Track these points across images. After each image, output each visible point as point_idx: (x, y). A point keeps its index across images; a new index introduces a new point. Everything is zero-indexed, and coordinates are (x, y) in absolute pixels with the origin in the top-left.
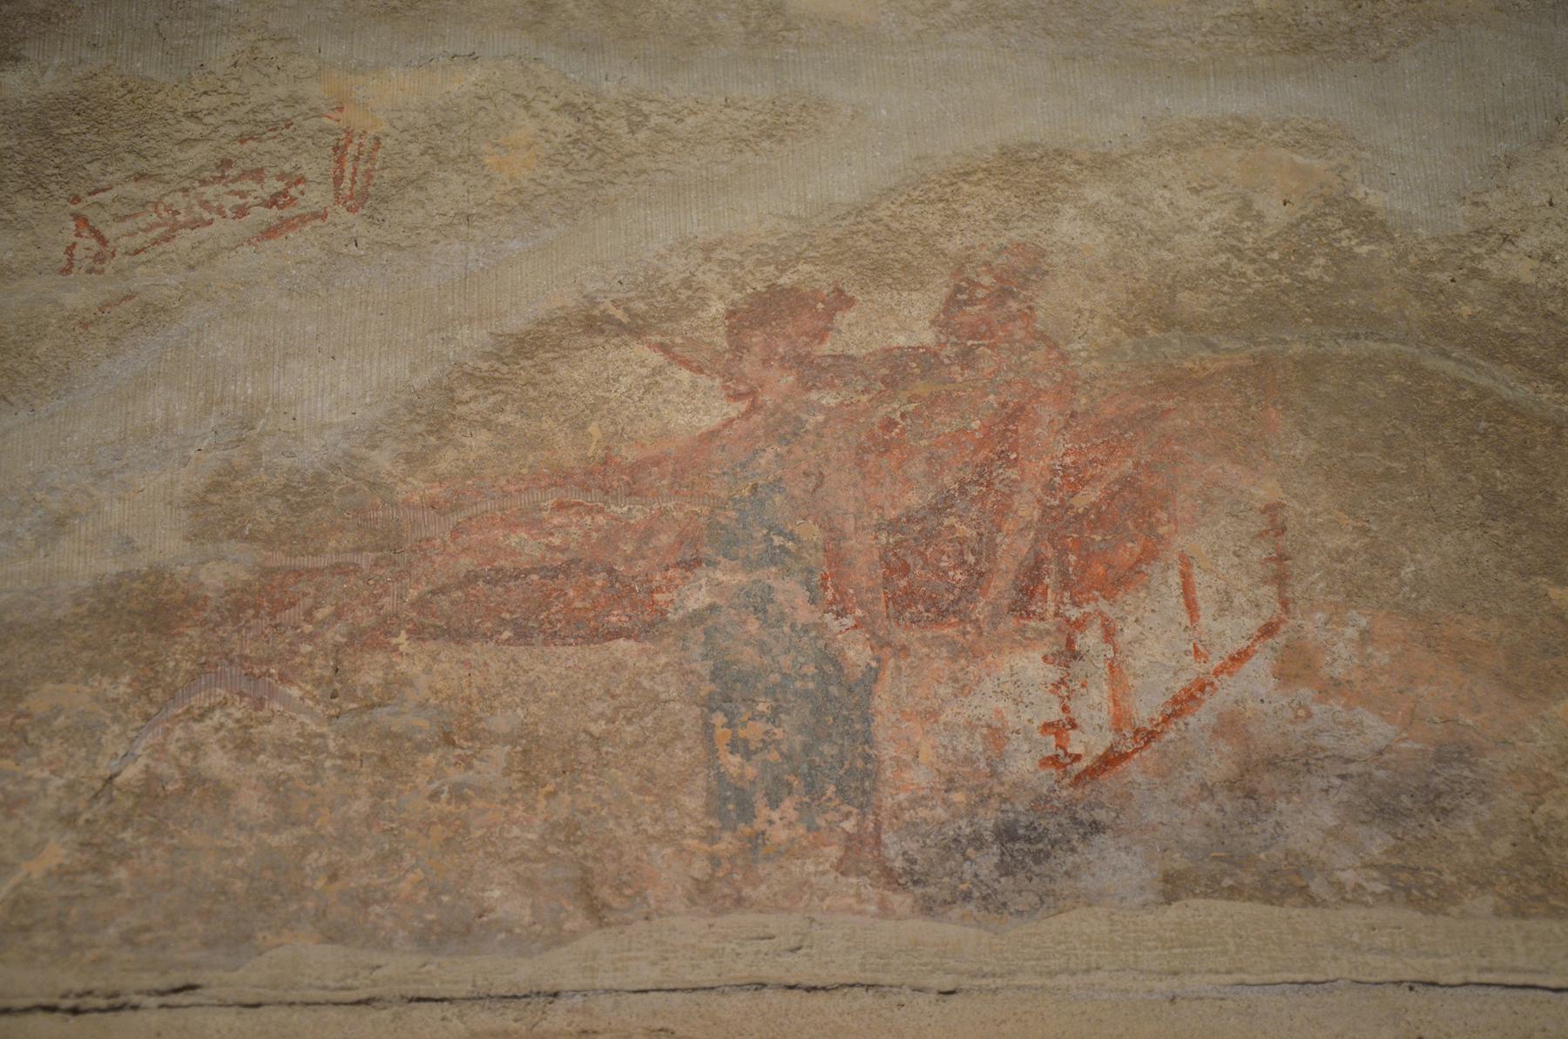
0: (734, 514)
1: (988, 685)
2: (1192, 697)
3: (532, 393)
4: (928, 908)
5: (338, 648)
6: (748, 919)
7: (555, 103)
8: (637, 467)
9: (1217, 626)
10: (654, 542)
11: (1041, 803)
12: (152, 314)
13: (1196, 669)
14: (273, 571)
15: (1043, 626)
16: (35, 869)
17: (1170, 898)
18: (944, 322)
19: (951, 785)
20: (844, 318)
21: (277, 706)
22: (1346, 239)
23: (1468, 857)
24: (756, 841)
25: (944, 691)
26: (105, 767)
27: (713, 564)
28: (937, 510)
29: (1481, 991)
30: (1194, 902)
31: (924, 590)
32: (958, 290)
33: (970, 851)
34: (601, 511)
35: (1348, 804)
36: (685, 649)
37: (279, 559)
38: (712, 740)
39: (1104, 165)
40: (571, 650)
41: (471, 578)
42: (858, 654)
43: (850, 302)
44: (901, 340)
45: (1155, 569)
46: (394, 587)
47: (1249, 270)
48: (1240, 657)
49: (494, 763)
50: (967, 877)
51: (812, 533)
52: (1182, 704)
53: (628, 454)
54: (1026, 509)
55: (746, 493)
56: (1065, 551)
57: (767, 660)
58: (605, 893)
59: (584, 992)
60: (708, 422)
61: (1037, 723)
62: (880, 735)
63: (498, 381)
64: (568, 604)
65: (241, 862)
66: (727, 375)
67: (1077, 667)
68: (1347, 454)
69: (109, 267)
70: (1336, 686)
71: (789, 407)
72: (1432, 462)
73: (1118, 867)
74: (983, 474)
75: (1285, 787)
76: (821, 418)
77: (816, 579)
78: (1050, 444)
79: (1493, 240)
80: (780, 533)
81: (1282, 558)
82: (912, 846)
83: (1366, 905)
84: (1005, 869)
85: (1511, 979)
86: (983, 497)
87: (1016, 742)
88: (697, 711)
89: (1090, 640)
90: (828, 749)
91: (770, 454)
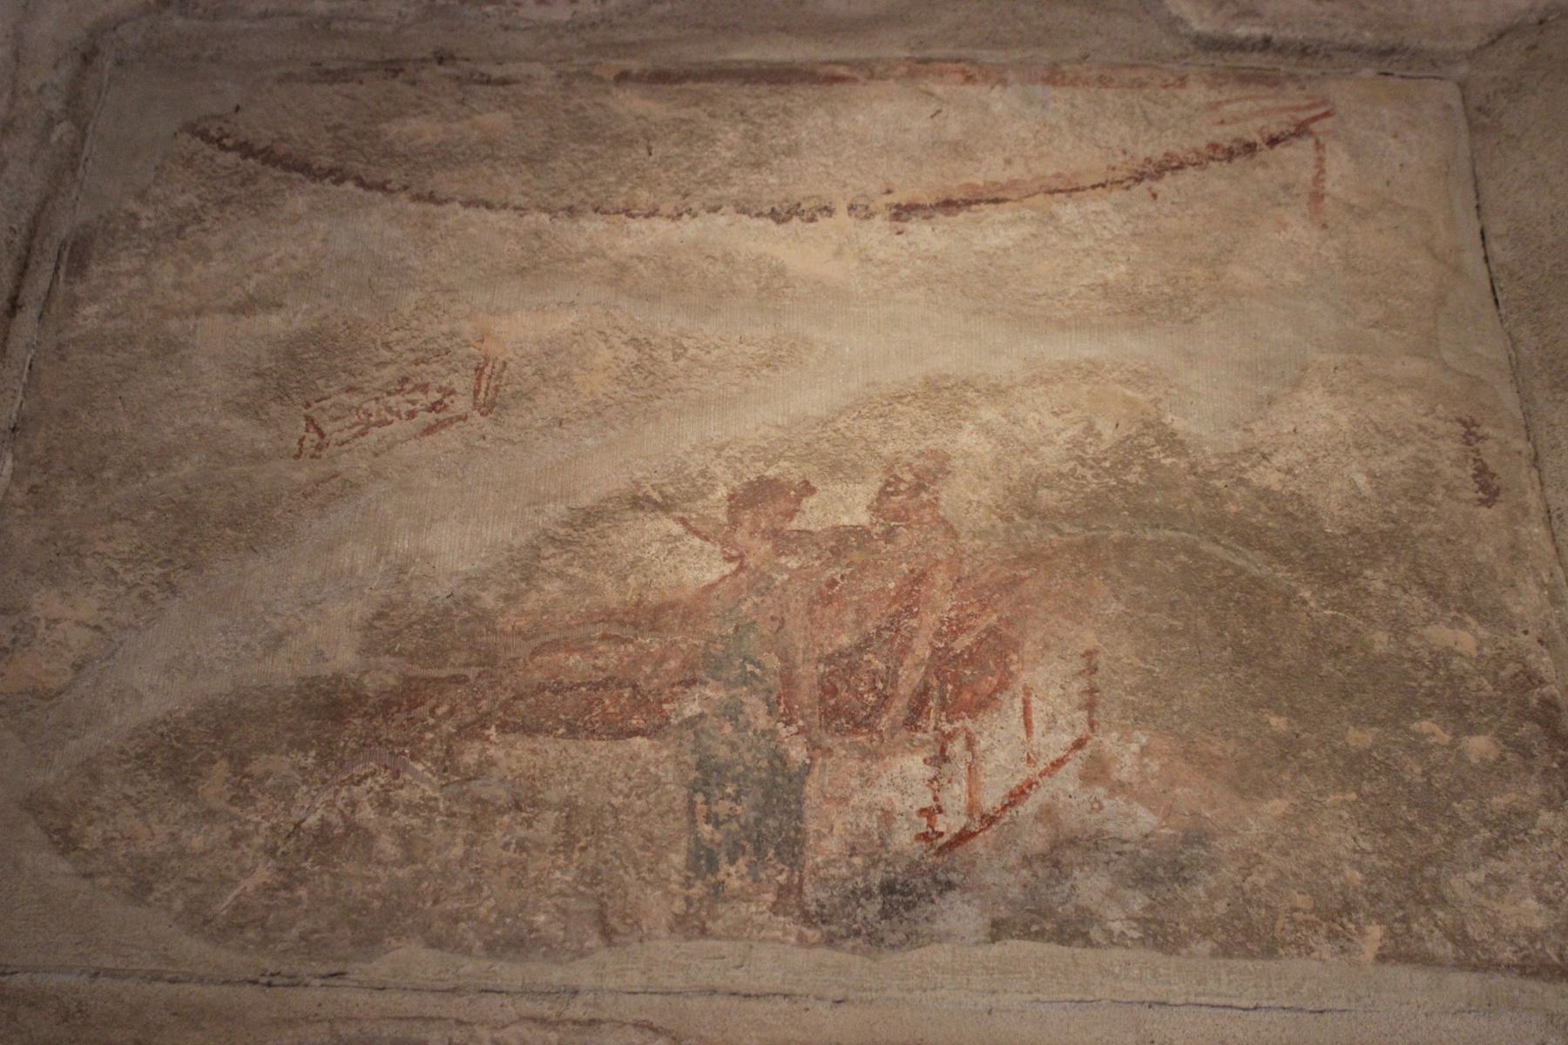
0: (720, 647)
1: (884, 781)
2: (1023, 792)
3: (593, 553)
4: (830, 941)
5: (450, 736)
6: (711, 943)
7: (625, 338)
8: (659, 610)
9: (1043, 741)
10: (666, 666)
11: (913, 867)
12: (350, 488)
13: (1030, 772)
14: (411, 679)
15: (926, 737)
17: (994, 938)
18: (876, 508)
19: (853, 851)
20: (809, 502)
21: (408, 777)
22: (1156, 453)
23: (1197, 913)
24: (718, 888)
25: (855, 782)
26: (297, 814)
27: (705, 684)
28: (860, 649)
29: (1196, 1009)
30: (1010, 942)
31: (848, 708)
32: (888, 484)
33: (862, 900)
34: (631, 642)
35: (1121, 873)
36: (680, 745)
37: (417, 670)
38: (693, 813)
39: (996, 392)
40: (603, 743)
41: (541, 688)
42: (797, 753)
43: (812, 491)
45: (1005, 697)
46: (489, 693)
47: (1089, 474)
48: (1058, 764)
49: (546, 826)
50: (859, 919)
51: (773, 663)
52: (1017, 796)
53: (652, 598)
54: (922, 649)
55: (731, 631)
56: (943, 683)
57: (735, 756)
58: (614, 921)
59: (595, 991)
60: (711, 577)
61: (916, 808)
62: (807, 814)
63: (570, 543)
64: (604, 710)
65: (378, 887)
67: (946, 768)
68: (1143, 614)
69: (324, 454)
71: (765, 568)
72: (1202, 622)
73: (961, 915)
74: (894, 624)
75: (1080, 859)
76: (786, 577)
77: (774, 697)
78: (942, 602)
80: (752, 662)
81: (1093, 691)
82: (822, 895)
83: (1127, 947)
84: (885, 914)
85: (1217, 1001)
86: (892, 640)
87: (900, 822)
88: (685, 791)
89: (957, 747)
90: (771, 822)
91: (749, 603)
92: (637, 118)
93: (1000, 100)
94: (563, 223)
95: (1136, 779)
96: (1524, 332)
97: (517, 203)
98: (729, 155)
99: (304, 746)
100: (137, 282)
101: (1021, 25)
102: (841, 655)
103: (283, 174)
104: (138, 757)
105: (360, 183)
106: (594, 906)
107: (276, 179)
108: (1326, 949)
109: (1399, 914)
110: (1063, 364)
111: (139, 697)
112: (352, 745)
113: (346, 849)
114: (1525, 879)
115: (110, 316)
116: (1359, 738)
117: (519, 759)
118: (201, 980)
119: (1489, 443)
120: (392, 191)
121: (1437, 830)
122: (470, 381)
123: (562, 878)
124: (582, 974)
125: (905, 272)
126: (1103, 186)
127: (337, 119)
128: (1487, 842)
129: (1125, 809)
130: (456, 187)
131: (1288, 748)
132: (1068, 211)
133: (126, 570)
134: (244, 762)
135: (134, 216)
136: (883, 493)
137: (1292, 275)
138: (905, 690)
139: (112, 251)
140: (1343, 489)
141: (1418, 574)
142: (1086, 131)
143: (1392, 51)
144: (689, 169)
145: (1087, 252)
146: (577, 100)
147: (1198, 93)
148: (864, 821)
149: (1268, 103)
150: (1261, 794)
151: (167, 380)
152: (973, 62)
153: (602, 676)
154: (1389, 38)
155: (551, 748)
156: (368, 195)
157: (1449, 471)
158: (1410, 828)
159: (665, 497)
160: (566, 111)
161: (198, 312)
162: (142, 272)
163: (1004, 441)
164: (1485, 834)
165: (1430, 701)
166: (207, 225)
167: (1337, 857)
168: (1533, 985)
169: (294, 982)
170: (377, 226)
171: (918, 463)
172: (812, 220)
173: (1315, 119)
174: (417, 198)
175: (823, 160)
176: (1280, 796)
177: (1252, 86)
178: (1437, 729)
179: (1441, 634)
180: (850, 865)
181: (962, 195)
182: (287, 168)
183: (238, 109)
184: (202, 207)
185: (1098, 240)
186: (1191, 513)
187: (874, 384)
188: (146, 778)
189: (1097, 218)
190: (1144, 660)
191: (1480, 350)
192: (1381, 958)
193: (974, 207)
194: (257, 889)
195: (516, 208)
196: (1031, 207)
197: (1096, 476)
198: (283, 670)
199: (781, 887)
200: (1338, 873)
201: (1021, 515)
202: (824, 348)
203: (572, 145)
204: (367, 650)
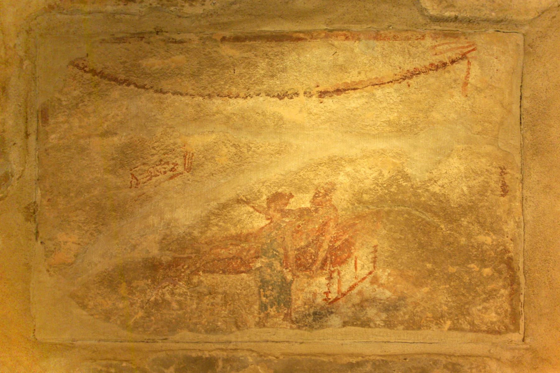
0: (266, 246)
1: (314, 284)
4: (299, 328)
5: (189, 274)
6: (265, 329)
7: (231, 144)
8: (248, 235)
9: (360, 272)
11: (322, 308)
12: (149, 198)
13: (355, 281)
14: (175, 258)
16: (138, 316)
17: (344, 326)
18: (312, 202)
19: (305, 304)
20: (291, 200)
24: (268, 315)
25: (306, 285)
26: (148, 298)
27: (262, 257)
31: (303, 264)
32: (316, 194)
35: (380, 308)
37: (177, 255)
39: (352, 161)
41: (214, 260)
42: (289, 277)
43: (293, 196)
44: (303, 206)
45: (349, 260)
46: (199, 261)
47: (379, 188)
48: (364, 279)
51: (282, 251)
52: (352, 288)
53: (245, 231)
54: (325, 246)
55: (269, 241)
56: (332, 256)
58: (239, 324)
59: (236, 342)
60: (262, 225)
62: (292, 294)
63: (219, 215)
64: (233, 266)
66: (266, 214)
67: (332, 281)
68: (392, 234)
69: (139, 187)
70: (382, 285)
71: (279, 222)
72: (410, 236)
73: (335, 320)
76: (285, 224)
77: (282, 261)
79: (432, 182)
81: (375, 257)
82: (297, 316)
84: (314, 320)
85: (403, 341)
86: (317, 244)
87: (318, 296)
89: (335, 275)
90: (282, 297)
92: (230, 57)
93: (358, 47)
94: (207, 101)
95: (386, 283)
96: (528, 135)
97: (191, 93)
98: (262, 72)
99: (147, 278)
100: (66, 126)
101: (367, 13)
102: (302, 248)
103: (108, 82)
104: (99, 282)
105: (136, 86)
106: (234, 320)
107: (106, 84)
108: (435, 327)
109: (456, 318)
110: (374, 151)
111: (96, 265)
112: (161, 278)
113: (163, 306)
114: (493, 308)
115: (60, 139)
116: (452, 269)
117: (209, 280)
118: (128, 342)
119: (508, 175)
120: (147, 89)
121: (470, 295)
122: (182, 160)
123: (224, 313)
124: (232, 337)
125: (323, 118)
126: (392, 82)
127: (124, 59)
128: (484, 298)
129: (382, 291)
130: (169, 87)
131: (431, 273)
132: (379, 92)
133: (85, 226)
134: (130, 283)
135: (59, 99)
136: (314, 197)
137: (453, 116)
138: (320, 259)
139: (55, 114)
140: (458, 192)
141: (478, 219)
142: (387, 60)
143: (502, 21)
144: (249, 78)
145: (384, 108)
146: (208, 50)
147: (429, 42)
148: (308, 296)
149: (453, 45)
150: (421, 286)
151: (84, 162)
152: (348, 31)
153: (231, 256)
154: (501, 15)
155: (219, 277)
156: (140, 90)
157: (493, 184)
158: (463, 295)
159: (247, 199)
160: (204, 54)
161: (90, 136)
162: (67, 122)
163: (353, 178)
164: (484, 296)
165: (475, 258)
166: (86, 103)
167: (441, 303)
168: (490, 336)
169: (154, 341)
170: (143, 102)
171: (326, 186)
172: (292, 98)
173: (469, 52)
174: (156, 91)
175: (295, 74)
176: (427, 287)
177: (448, 38)
178: (475, 266)
179: (482, 238)
180: (304, 308)
181: (343, 87)
182: (110, 80)
183: (87, 55)
184: (83, 96)
185: (388, 103)
186: (410, 201)
187: (312, 159)
188: (102, 288)
189: (390, 93)
190: (391, 248)
191: (511, 141)
192: (450, 329)
193: (347, 92)
194: (140, 317)
195: (191, 95)
196: (367, 92)
197: (381, 189)
198: (138, 255)
199: (285, 314)
200: (440, 307)
201: (357, 203)
202: (296, 147)
203: (208, 69)
204: (161, 249)
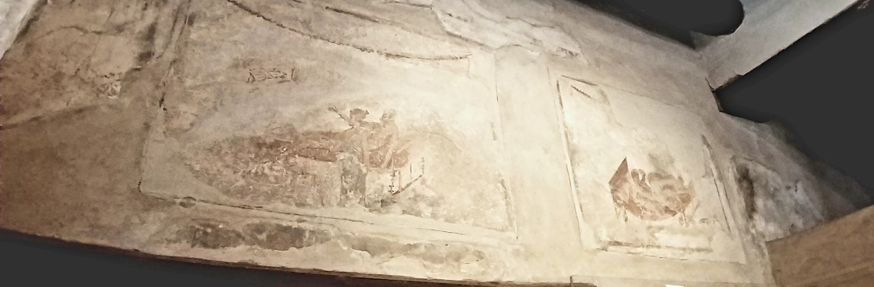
4: (370, 211)
8: (335, 134)
11: (388, 197)
28: (378, 149)
37: (278, 139)
42: (364, 170)
51: (359, 149)
52: (408, 185)
54: (390, 152)
70: (427, 186)
73: (396, 208)
74: (385, 146)
84: (382, 206)
89: (397, 174)
94: (313, 40)
108: (463, 221)
169: (250, 208)
